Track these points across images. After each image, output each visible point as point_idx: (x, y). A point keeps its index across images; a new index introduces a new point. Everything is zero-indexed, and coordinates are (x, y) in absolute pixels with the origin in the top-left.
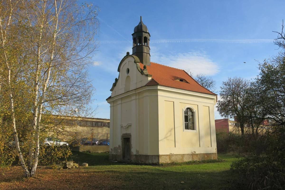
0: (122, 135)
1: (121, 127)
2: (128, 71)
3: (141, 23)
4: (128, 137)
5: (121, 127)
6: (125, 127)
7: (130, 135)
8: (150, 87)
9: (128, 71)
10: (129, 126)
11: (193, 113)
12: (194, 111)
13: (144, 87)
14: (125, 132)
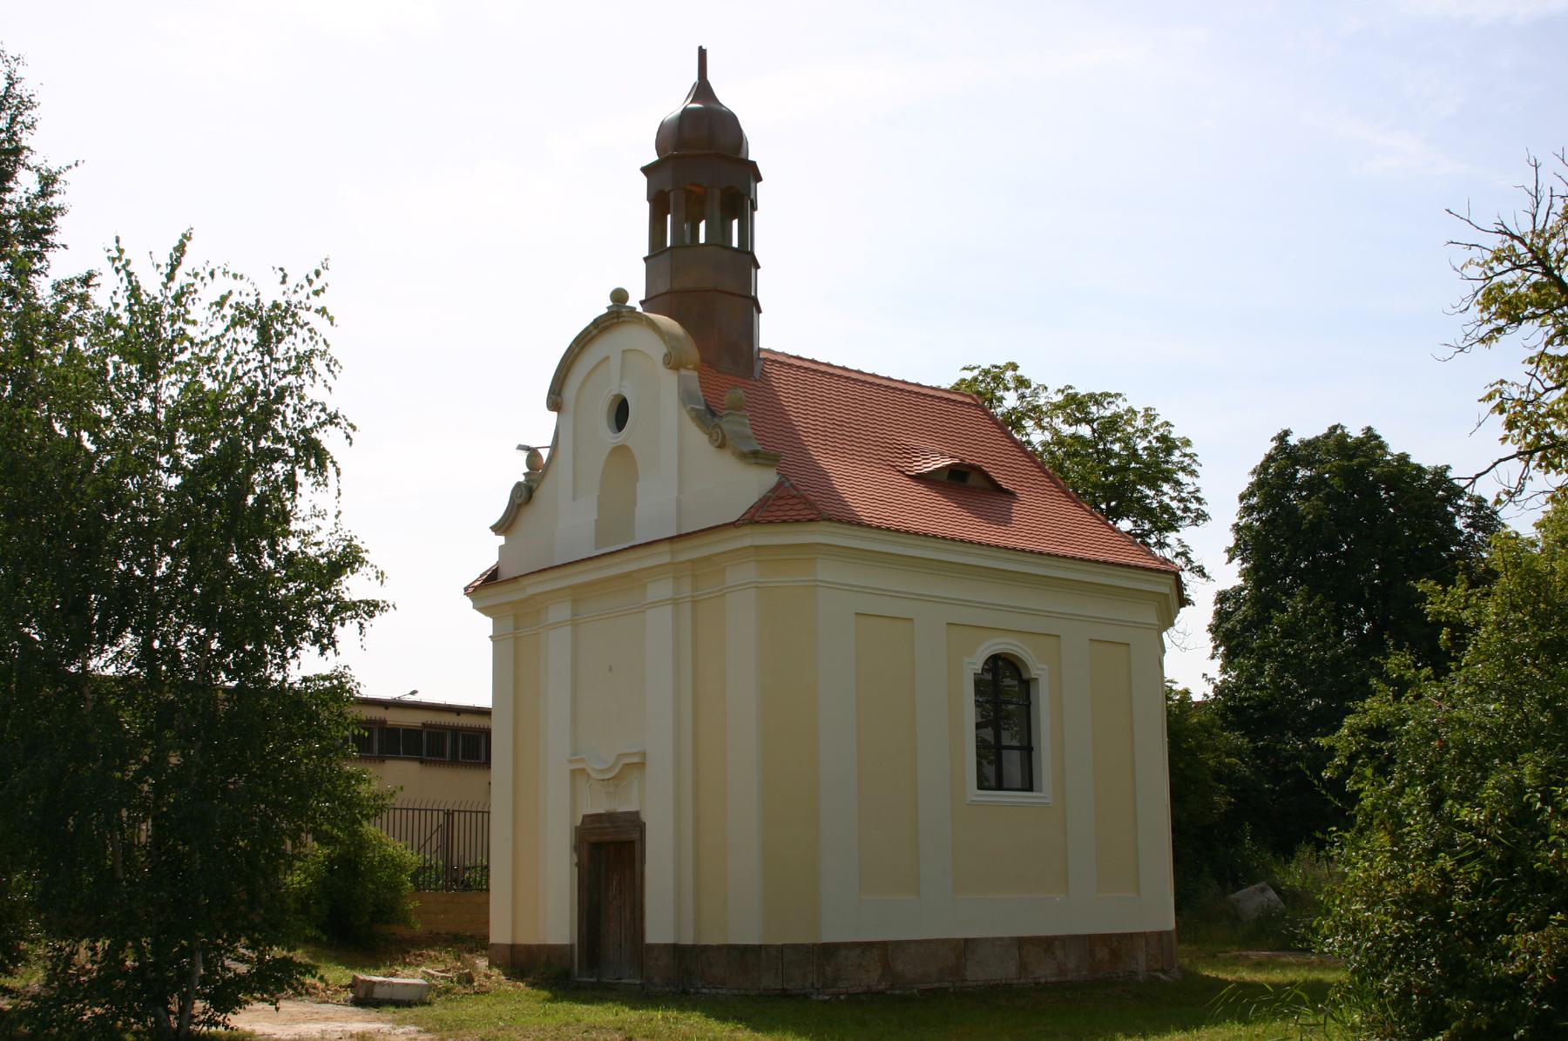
0: (579, 822)
1: (573, 772)
2: (621, 413)
3: (703, 89)
4: (624, 837)
5: (573, 772)
6: (602, 771)
7: (634, 823)
8: (771, 528)
9: (621, 413)
10: (635, 766)
11: (1026, 684)
12: (1034, 673)
13: (734, 532)
14: (599, 805)
